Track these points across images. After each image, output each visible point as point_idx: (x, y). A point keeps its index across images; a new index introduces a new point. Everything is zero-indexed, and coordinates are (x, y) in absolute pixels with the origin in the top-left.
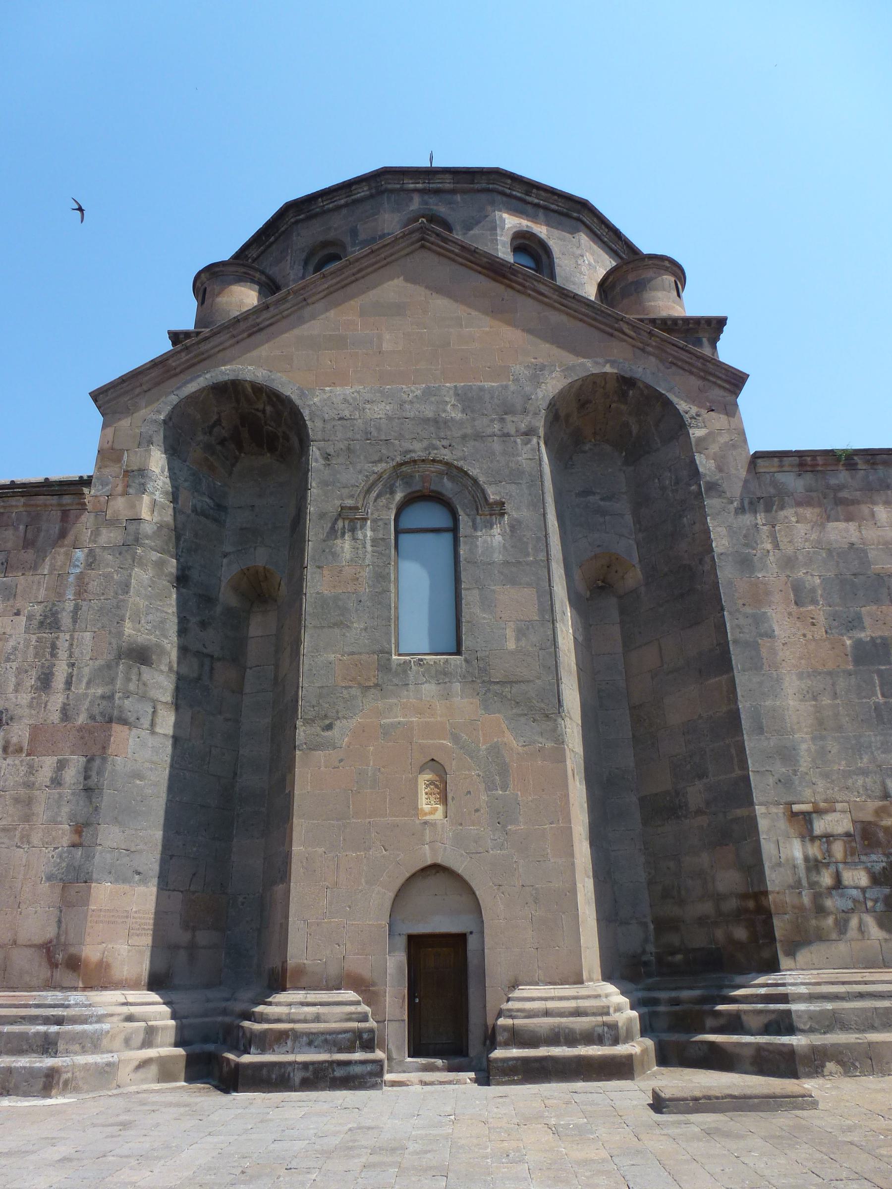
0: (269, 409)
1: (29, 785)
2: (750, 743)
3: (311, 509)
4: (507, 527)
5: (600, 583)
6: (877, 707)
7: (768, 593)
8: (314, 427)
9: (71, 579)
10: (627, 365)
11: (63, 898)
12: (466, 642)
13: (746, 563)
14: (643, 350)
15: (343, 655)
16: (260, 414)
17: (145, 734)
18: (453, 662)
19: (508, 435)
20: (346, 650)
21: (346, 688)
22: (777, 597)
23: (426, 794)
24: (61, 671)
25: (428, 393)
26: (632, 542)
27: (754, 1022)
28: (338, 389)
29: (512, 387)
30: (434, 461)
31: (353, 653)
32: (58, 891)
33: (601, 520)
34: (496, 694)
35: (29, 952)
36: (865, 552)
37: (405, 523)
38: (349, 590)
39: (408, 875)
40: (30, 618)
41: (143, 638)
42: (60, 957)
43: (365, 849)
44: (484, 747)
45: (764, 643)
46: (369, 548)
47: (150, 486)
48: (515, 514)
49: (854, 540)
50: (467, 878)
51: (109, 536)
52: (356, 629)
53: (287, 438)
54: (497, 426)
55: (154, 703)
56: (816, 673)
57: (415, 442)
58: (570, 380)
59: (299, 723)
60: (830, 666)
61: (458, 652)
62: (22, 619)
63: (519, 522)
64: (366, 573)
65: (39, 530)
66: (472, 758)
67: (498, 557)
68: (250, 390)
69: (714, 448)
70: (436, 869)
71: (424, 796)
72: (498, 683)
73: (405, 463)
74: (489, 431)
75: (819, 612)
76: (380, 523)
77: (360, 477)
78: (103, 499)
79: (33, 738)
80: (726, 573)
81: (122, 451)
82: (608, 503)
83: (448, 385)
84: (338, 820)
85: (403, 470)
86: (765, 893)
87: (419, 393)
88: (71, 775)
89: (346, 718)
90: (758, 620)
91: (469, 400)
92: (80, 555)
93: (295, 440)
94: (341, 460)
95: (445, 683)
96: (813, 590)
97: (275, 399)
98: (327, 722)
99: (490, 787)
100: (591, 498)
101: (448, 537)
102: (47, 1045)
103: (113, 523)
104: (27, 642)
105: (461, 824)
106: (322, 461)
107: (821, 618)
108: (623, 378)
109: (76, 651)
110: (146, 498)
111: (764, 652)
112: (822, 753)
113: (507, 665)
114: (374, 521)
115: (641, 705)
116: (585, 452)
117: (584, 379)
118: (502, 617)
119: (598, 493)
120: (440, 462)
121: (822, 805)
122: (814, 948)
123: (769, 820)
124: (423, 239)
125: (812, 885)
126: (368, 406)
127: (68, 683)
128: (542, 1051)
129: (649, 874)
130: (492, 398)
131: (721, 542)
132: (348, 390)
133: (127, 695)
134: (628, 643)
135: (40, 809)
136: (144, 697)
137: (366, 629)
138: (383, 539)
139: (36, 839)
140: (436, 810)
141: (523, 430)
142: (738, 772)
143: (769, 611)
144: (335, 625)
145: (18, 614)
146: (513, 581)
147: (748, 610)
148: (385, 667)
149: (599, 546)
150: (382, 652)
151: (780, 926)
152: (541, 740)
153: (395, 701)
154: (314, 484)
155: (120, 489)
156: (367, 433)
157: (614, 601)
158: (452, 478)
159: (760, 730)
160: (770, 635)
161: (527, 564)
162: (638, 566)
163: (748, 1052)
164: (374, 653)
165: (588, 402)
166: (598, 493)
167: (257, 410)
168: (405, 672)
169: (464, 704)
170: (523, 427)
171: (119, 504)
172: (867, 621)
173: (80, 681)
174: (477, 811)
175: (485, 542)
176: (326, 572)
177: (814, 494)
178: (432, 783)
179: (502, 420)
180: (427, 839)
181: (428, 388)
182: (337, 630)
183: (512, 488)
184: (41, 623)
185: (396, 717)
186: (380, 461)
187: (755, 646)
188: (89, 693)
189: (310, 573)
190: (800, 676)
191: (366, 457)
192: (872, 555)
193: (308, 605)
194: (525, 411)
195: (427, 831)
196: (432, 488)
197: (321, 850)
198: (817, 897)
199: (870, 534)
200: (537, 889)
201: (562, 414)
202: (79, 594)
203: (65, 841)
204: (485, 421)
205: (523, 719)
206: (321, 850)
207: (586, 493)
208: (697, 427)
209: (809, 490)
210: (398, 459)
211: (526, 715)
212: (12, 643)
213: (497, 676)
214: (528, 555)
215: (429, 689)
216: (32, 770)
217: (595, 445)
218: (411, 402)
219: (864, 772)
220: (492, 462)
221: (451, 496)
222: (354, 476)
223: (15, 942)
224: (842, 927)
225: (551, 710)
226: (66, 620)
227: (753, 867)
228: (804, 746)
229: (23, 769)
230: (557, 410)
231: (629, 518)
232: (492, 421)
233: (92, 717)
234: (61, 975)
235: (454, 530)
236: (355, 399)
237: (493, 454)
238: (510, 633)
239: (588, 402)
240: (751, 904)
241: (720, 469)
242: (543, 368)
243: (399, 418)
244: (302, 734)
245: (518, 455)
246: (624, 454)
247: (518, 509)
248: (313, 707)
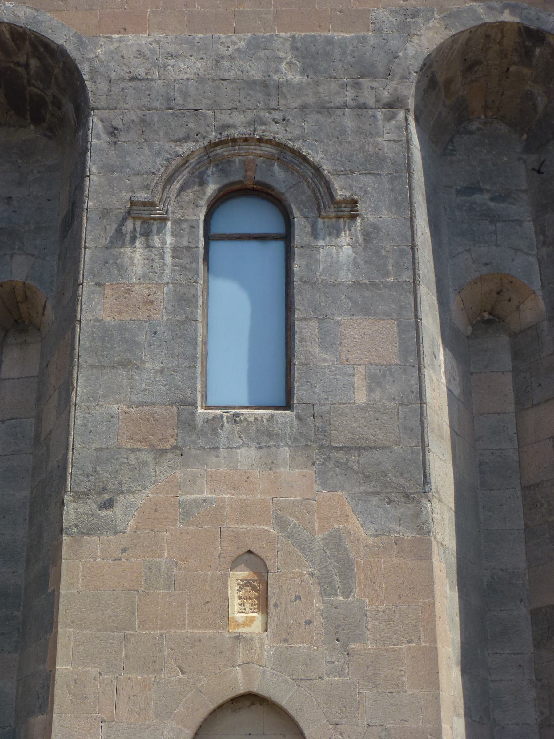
0: (34, 63)
3: (90, 203)
4: (359, 235)
5: (486, 316)
8: (96, 90)
10: (533, 13)
15: (130, 406)
16: (20, 70)
18: (280, 419)
19: (364, 107)
20: (134, 398)
21: (133, 451)
23: (240, 598)
25: (255, 45)
26: (534, 260)
28: (130, 36)
29: (372, 40)
30: (260, 140)
31: (143, 404)
33: (491, 228)
34: (338, 464)
37: (218, 228)
38: (140, 317)
39: (212, 707)
43: (155, 671)
44: (321, 536)
46: (169, 260)
48: (371, 218)
50: (293, 712)
52: (148, 371)
53: (58, 105)
54: (349, 94)
57: (235, 113)
58: (453, 32)
59: (68, 498)
61: (288, 406)
63: (376, 228)
64: (164, 294)
66: (303, 550)
67: (345, 276)
68: (8, 35)
70: (251, 699)
71: (237, 601)
72: (341, 449)
73: (220, 143)
74: (338, 100)
76: (185, 226)
77: (158, 161)
82: (501, 205)
83: (283, 34)
84: (118, 630)
85: (217, 152)
87: (242, 44)
89: (133, 493)
91: (311, 57)
93: (69, 108)
94: (133, 136)
95: (269, 447)
97: (42, 50)
98: (106, 497)
99: (327, 590)
100: (478, 198)
101: (278, 247)
105: (286, 641)
106: (105, 137)
108: (528, 30)
113: (355, 425)
114: (177, 222)
115: (538, 485)
116: (471, 133)
117: (473, 31)
118: (349, 358)
119: (488, 191)
120: (269, 142)
126: (171, 62)
129: (542, 713)
130: (344, 53)
132: (144, 39)
134: (523, 400)
137: (162, 371)
138: (188, 248)
140: (252, 620)
141: (385, 100)
144: (122, 364)
146: (366, 311)
148: (187, 423)
149: (486, 264)
150: (183, 402)
152: (398, 528)
153: (199, 470)
154: (94, 169)
156: (169, 99)
157: (505, 339)
158: (285, 165)
161: (386, 286)
162: (540, 293)
164: (172, 404)
165: (477, 63)
166: (488, 191)
167: (18, 64)
168: (214, 431)
169: (294, 477)
170: (386, 95)
174: (308, 622)
175: (329, 254)
176: (108, 292)
178: (247, 583)
179: (357, 86)
180: (240, 660)
181: (255, 38)
182: (122, 372)
183: (368, 181)
185: (201, 492)
186: (186, 139)
189: (87, 291)
191: (166, 133)
195: (240, 649)
196: (258, 178)
197: (94, 670)
200: (387, 730)
201: (441, 79)
204: (334, 86)
205: (374, 500)
206: (94, 670)
207: (472, 189)
210: (212, 137)
211: (378, 493)
213: (340, 438)
214: (387, 274)
215: (247, 455)
217: (485, 123)
218: (232, 58)
220: (341, 144)
221: (283, 190)
222: (149, 159)
230: (433, 74)
231: (529, 226)
232: (343, 86)
235: (287, 237)
236: (153, 51)
237: (343, 132)
238: (360, 382)
239: (477, 63)
242: (415, 14)
243: (213, 80)
244: (72, 512)
245: (378, 135)
246: (525, 137)
247: (376, 210)
248: (88, 477)
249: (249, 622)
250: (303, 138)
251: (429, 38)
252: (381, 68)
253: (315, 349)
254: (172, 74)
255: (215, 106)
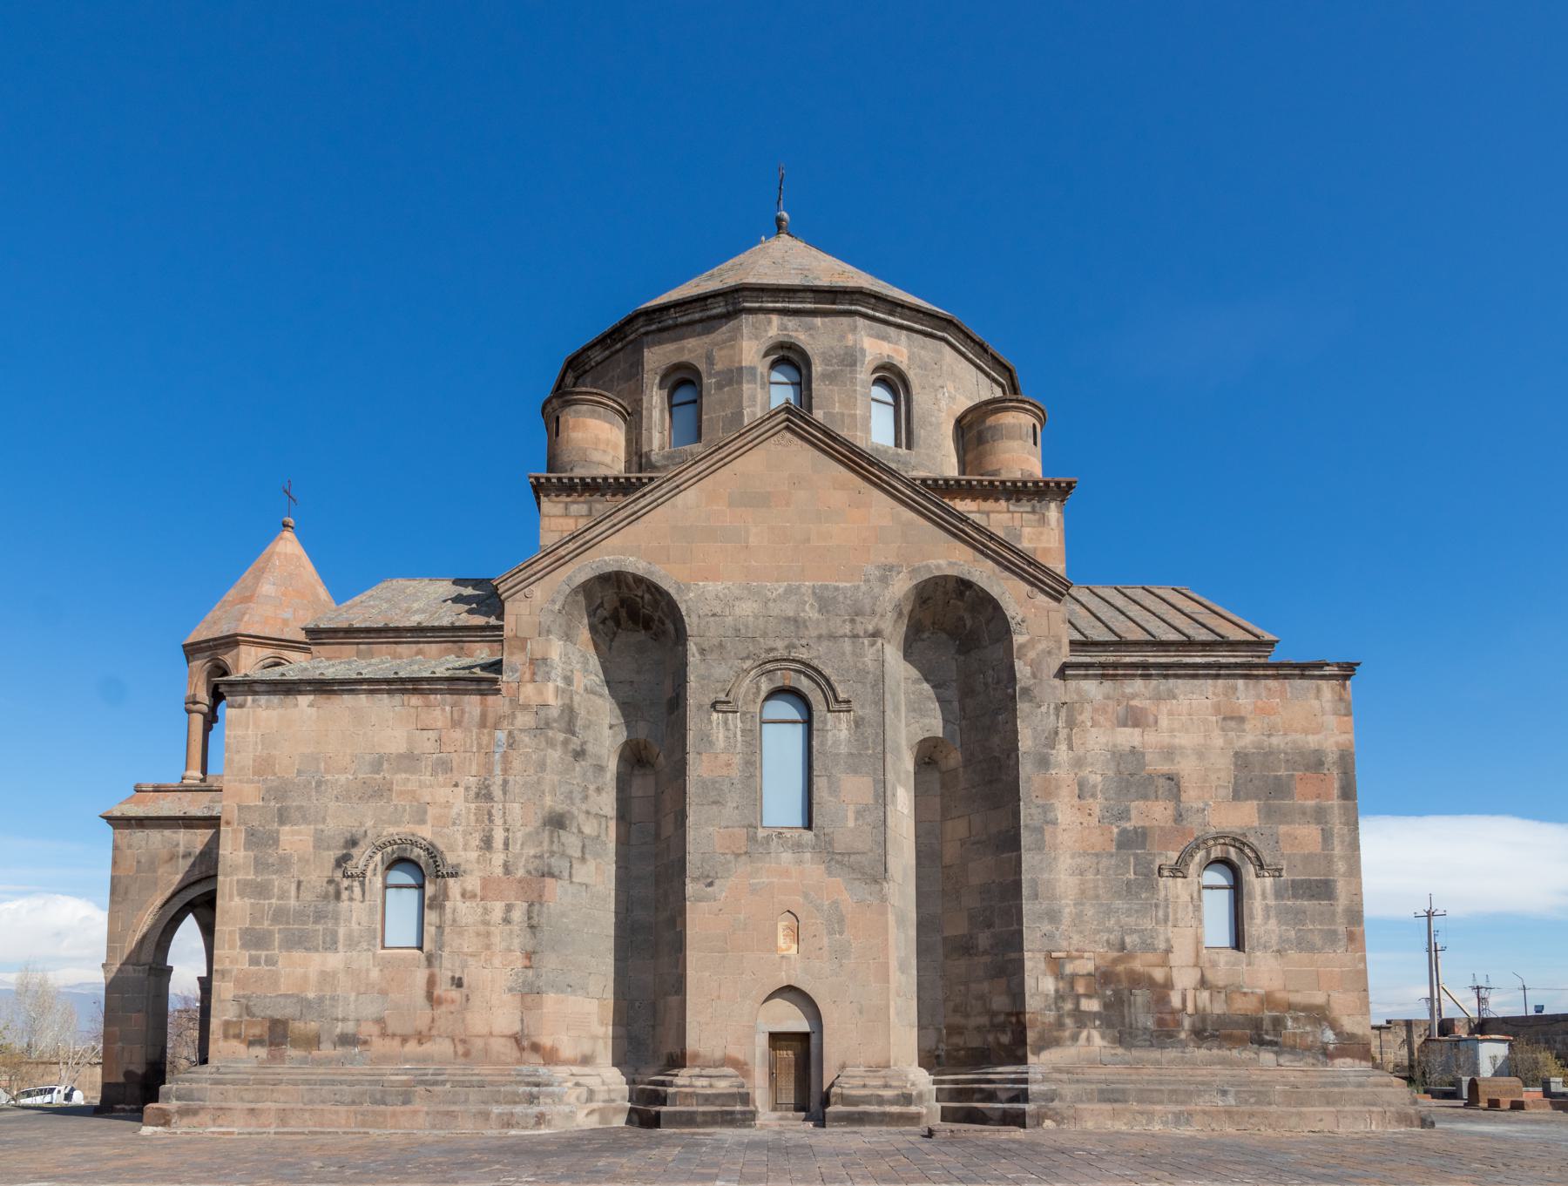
0: (647, 596)
1: (486, 923)
2: (1027, 906)
3: (691, 701)
6: (1128, 883)
7: (1058, 787)
8: (691, 623)
9: (497, 756)
11: (522, 1002)
12: (816, 820)
13: (1044, 762)
14: (982, 552)
17: (566, 883)
19: (856, 636)
22: (1064, 792)
24: (499, 836)
25: (789, 591)
27: (1003, 1096)
29: (864, 588)
32: (518, 998)
35: (503, 1040)
36: (1143, 754)
37: (766, 716)
40: (467, 789)
41: (561, 807)
42: (525, 1043)
45: (1048, 829)
47: (553, 675)
49: (1136, 744)
51: (524, 720)
54: (847, 628)
55: (570, 857)
56: (1085, 854)
59: (688, 881)
60: (1098, 849)
62: (461, 790)
64: (737, 760)
65: (463, 712)
69: (1032, 655)
74: (841, 632)
75: (1096, 805)
78: (515, 685)
79: (484, 887)
80: (1026, 769)
81: (525, 639)
85: (767, 665)
86: (1024, 1013)
87: (781, 590)
88: (518, 915)
90: (1046, 809)
91: (825, 602)
92: (501, 735)
94: (715, 656)
96: (1095, 786)
99: (831, 933)
102: (532, 1099)
103: (526, 707)
104: (469, 812)
107: (1097, 811)
109: (509, 819)
110: (551, 685)
111: (1047, 837)
112: (1080, 915)
114: (744, 714)
118: (846, 795)
121: (1075, 954)
122: (1053, 1050)
123: (1033, 963)
124: (788, 420)
125: (1058, 1009)
127: (506, 845)
128: (861, 1108)
131: (1026, 742)
132: (720, 586)
133: (552, 854)
135: (496, 939)
136: (563, 855)
139: (497, 962)
142: (1015, 927)
143: (1057, 805)
144: (714, 803)
145: (456, 785)
146: (855, 770)
147: (1040, 801)
148: (752, 839)
151: (1031, 1036)
155: (527, 676)
159: (1036, 897)
160: (1054, 823)
163: (997, 1115)
169: (813, 870)
170: (870, 628)
171: (528, 691)
172: (1133, 813)
173: (515, 843)
176: (704, 757)
177: (1110, 702)
179: (852, 621)
184: (477, 795)
186: (748, 657)
187: (1041, 831)
188: (525, 855)
190: (1073, 857)
192: (1148, 758)
193: (692, 787)
194: (873, 613)
198: (1060, 1018)
199: (1152, 738)
202: (505, 771)
203: (519, 963)
204: (839, 621)
208: (1021, 633)
209: (1107, 697)
212: (454, 811)
215: (787, 857)
216: (486, 911)
219: (1110, 931)
223: (491, 1034)
224: (1075, 1038)
225: (877, 875)
226: (497, 792)
227: (1018, 995)
228: (1067, 910)
229: (480, 910)
233: (529, 872)
234: (527, 1055)
235: (808, 722)
237: (843, 654)
238: (851, 815)
240: (1014, 1019)
241: (1034, 676)
242: (891, 568)
249: (789, 948)
250: (819, 657)
251: (901, 586)
252: (868, 610)
253: (825, 794)
254: (737, 611)
255: (765, 635)
